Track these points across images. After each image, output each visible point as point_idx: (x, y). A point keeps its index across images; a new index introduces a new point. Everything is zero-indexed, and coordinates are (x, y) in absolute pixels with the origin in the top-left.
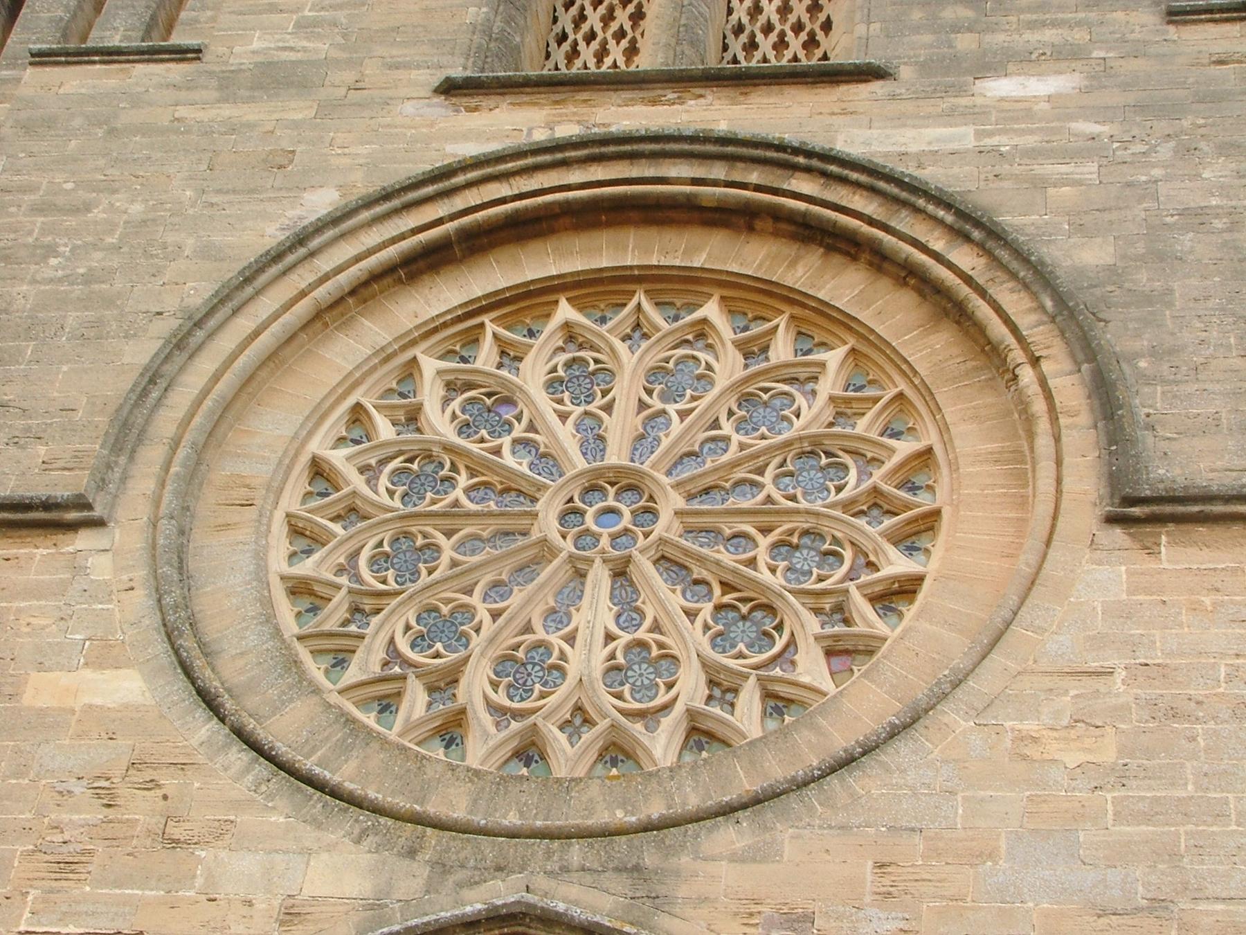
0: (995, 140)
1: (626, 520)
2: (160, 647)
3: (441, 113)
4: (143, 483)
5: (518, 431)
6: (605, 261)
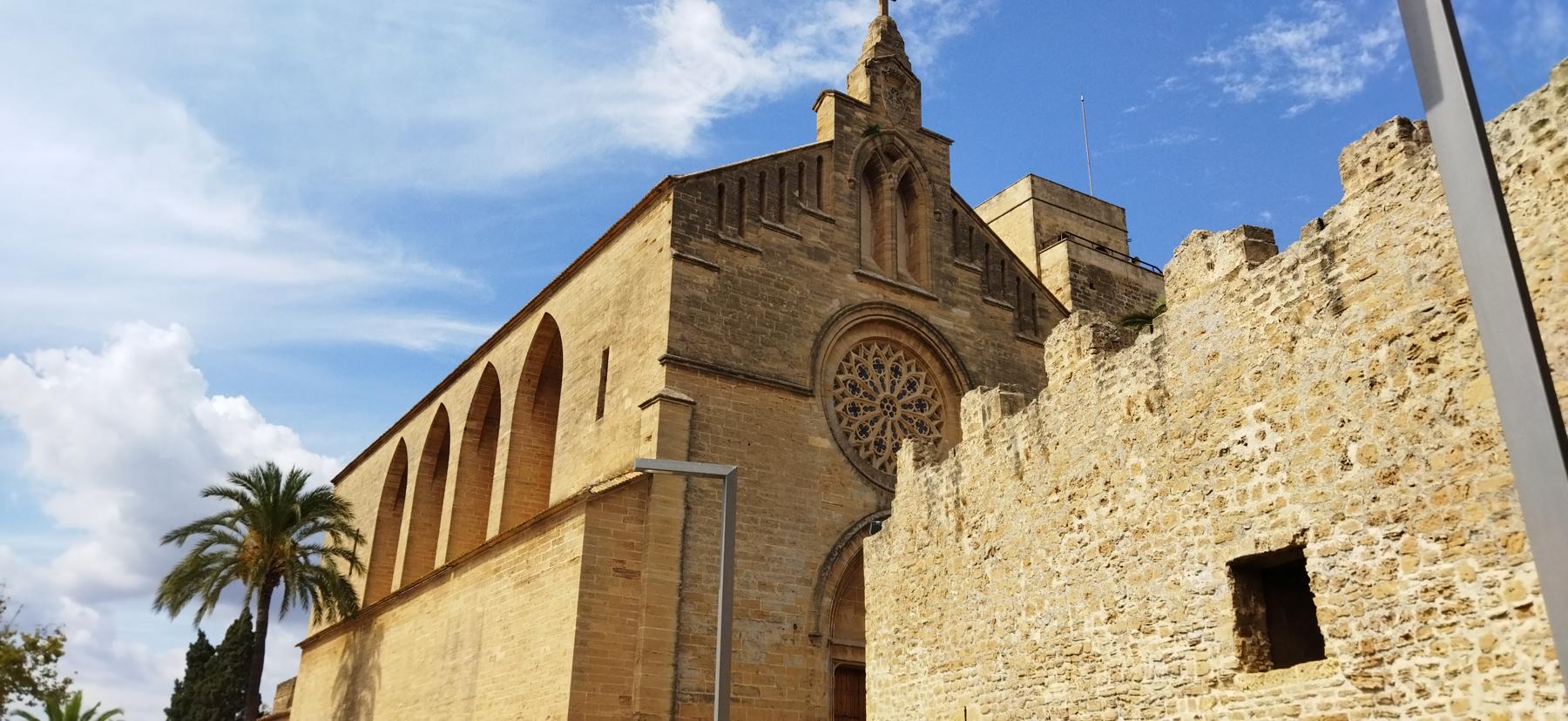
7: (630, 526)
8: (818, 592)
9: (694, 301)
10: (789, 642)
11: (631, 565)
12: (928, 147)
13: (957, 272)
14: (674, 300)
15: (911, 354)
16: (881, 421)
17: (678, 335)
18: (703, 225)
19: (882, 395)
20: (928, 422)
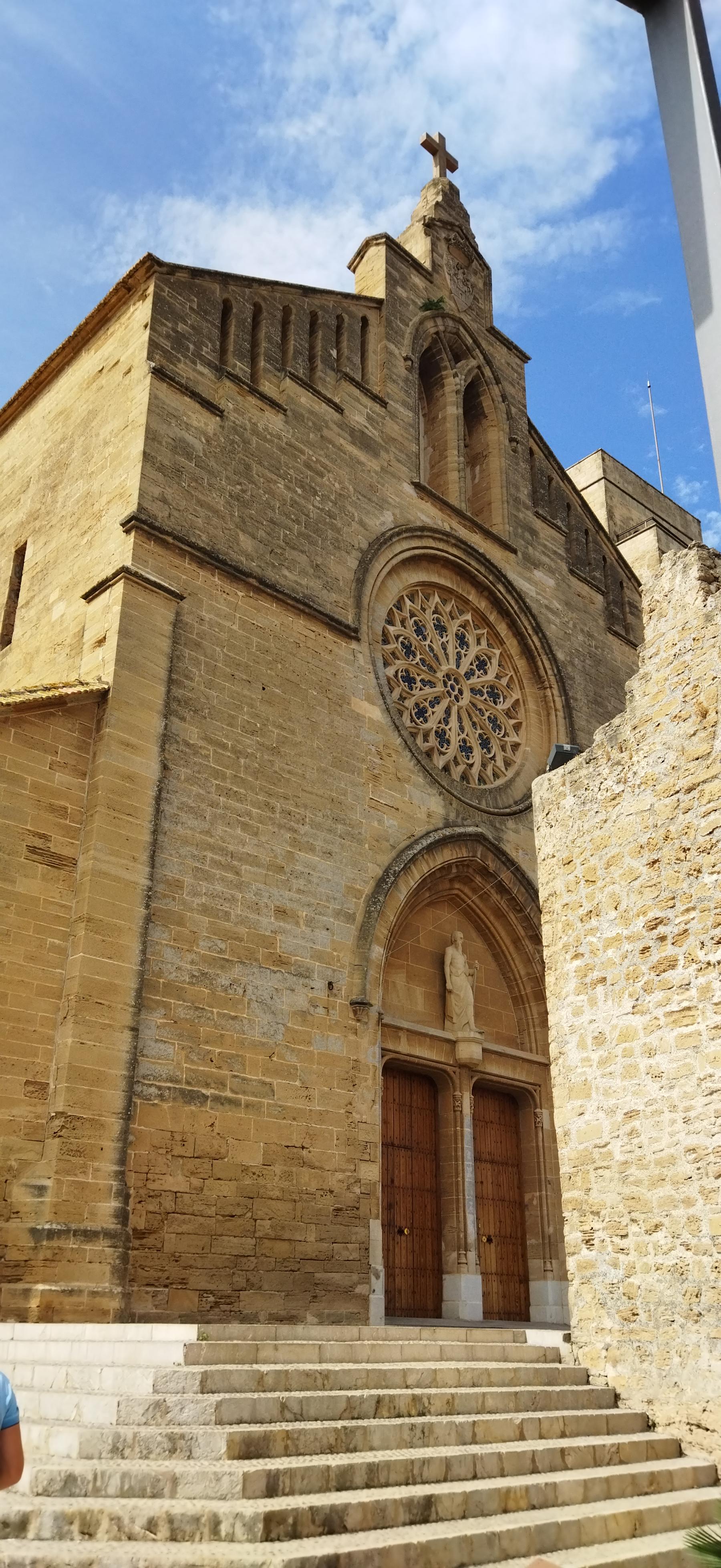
0: (539, 597)
2: (382, 702)
6: (449, 584)
7: (61, 778)
8: (364, 935)
9: (181, 448)
10: (321, 1011)
11: (59, 845)
12: (500, 355)
13: (538, 524)
14: (151, 436)
15: (482, 620)
17: (157, 491)
18: (199, 346)
19: (445, 668)
20: (502, 719)
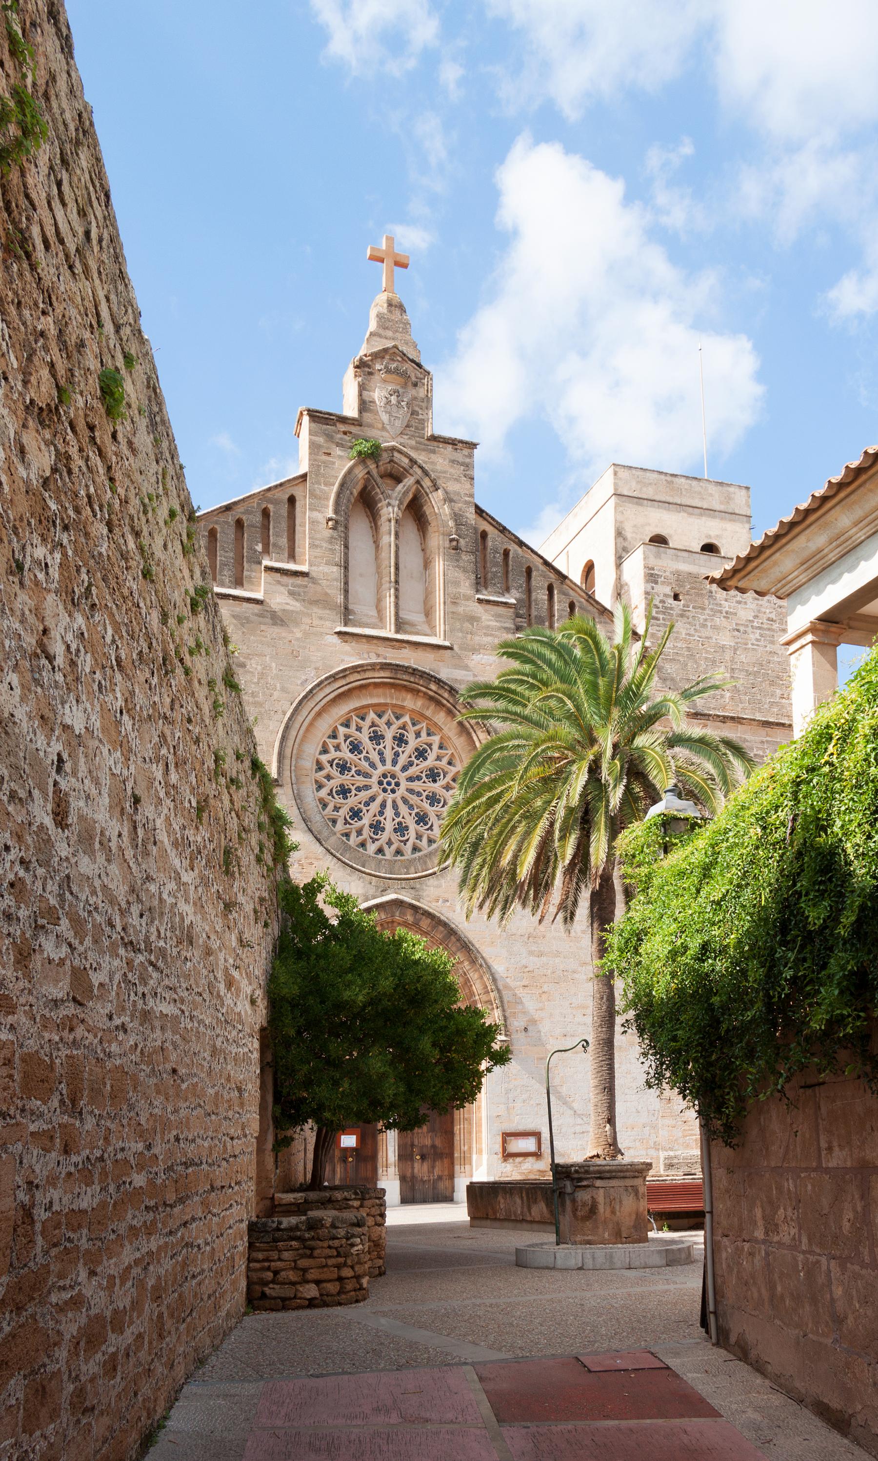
1: (393, 785)
3: (335, 639)
4: (287, 773)
5: (364, 754)
16: (379, 800)
